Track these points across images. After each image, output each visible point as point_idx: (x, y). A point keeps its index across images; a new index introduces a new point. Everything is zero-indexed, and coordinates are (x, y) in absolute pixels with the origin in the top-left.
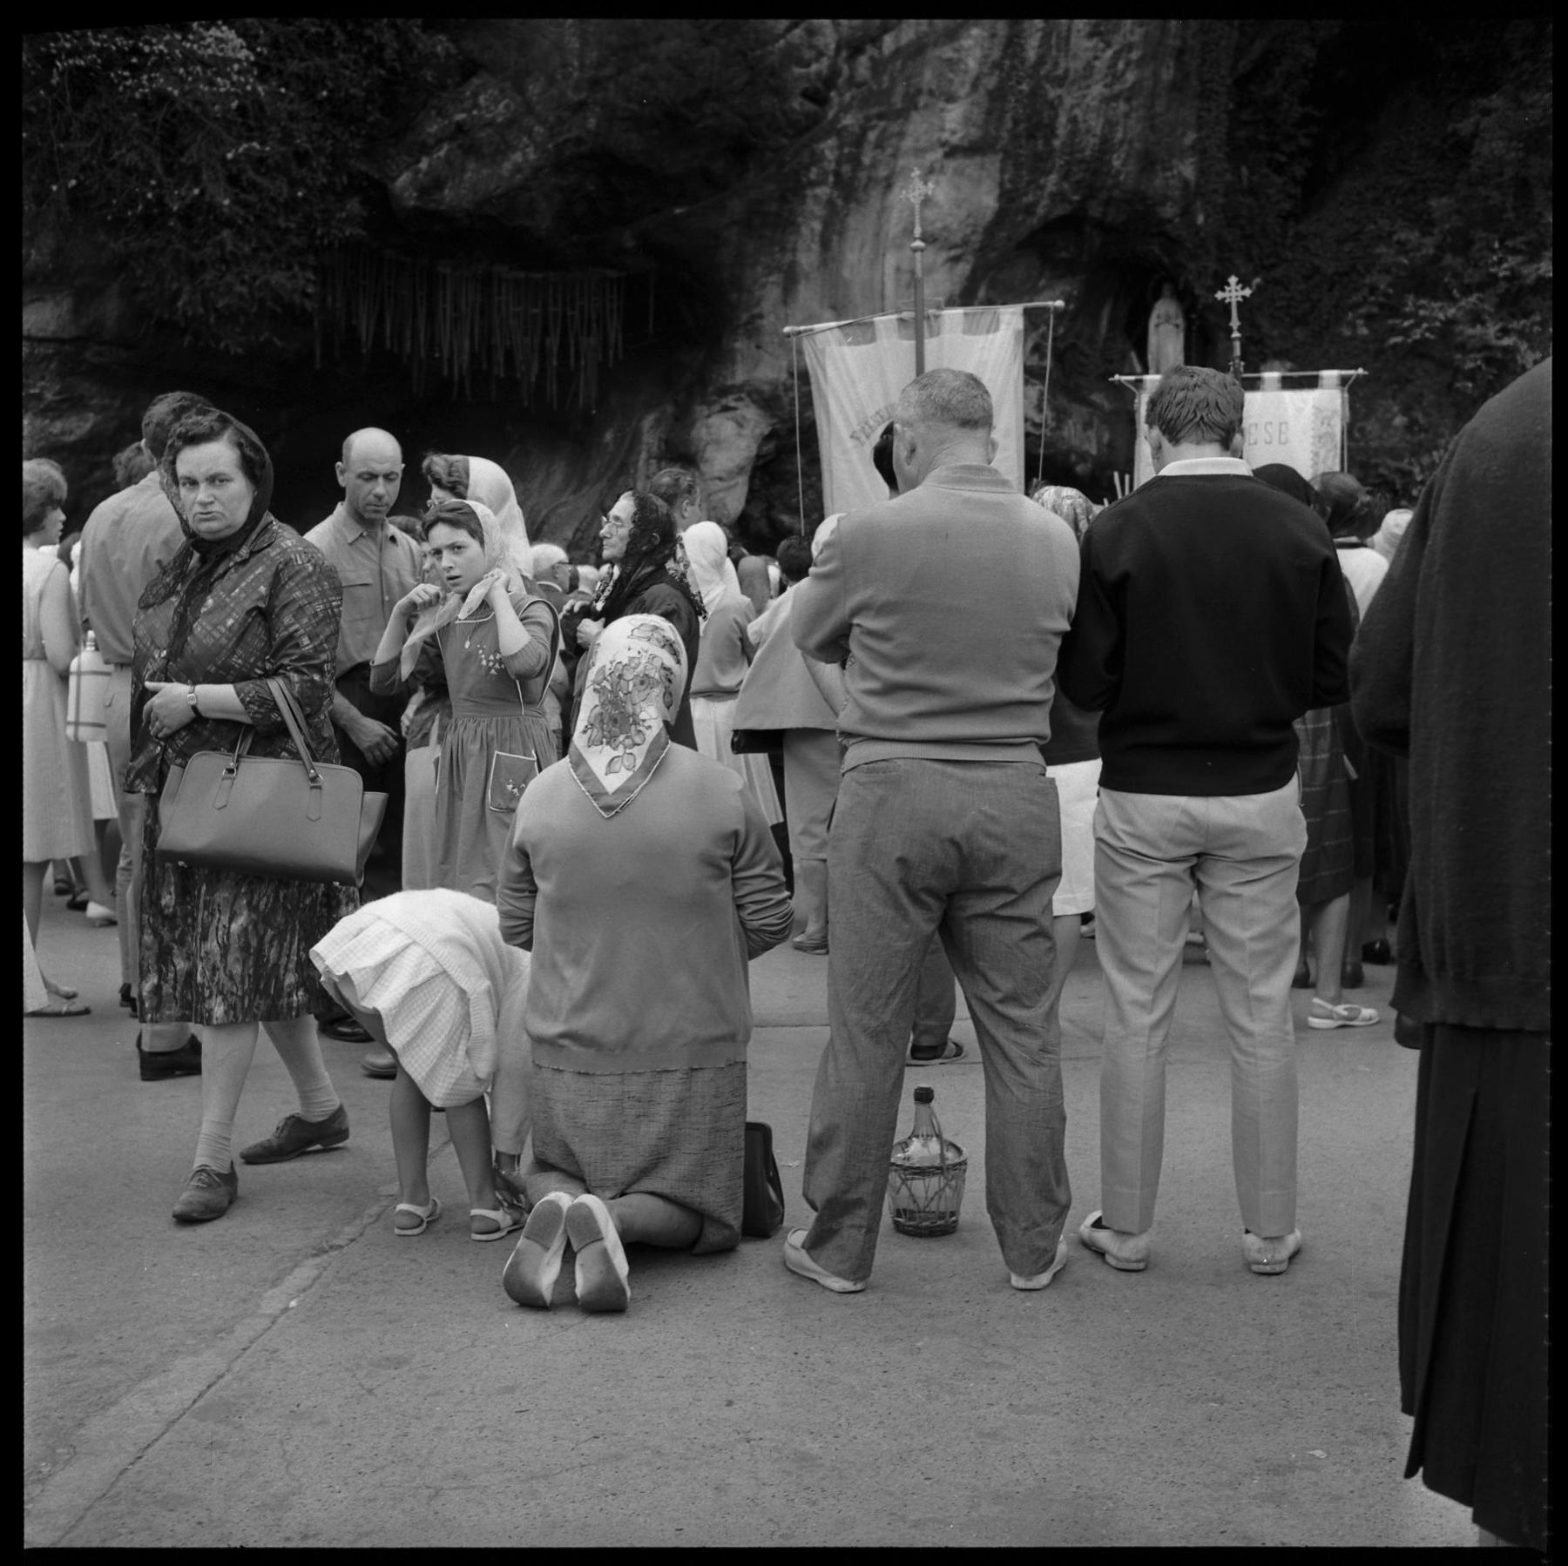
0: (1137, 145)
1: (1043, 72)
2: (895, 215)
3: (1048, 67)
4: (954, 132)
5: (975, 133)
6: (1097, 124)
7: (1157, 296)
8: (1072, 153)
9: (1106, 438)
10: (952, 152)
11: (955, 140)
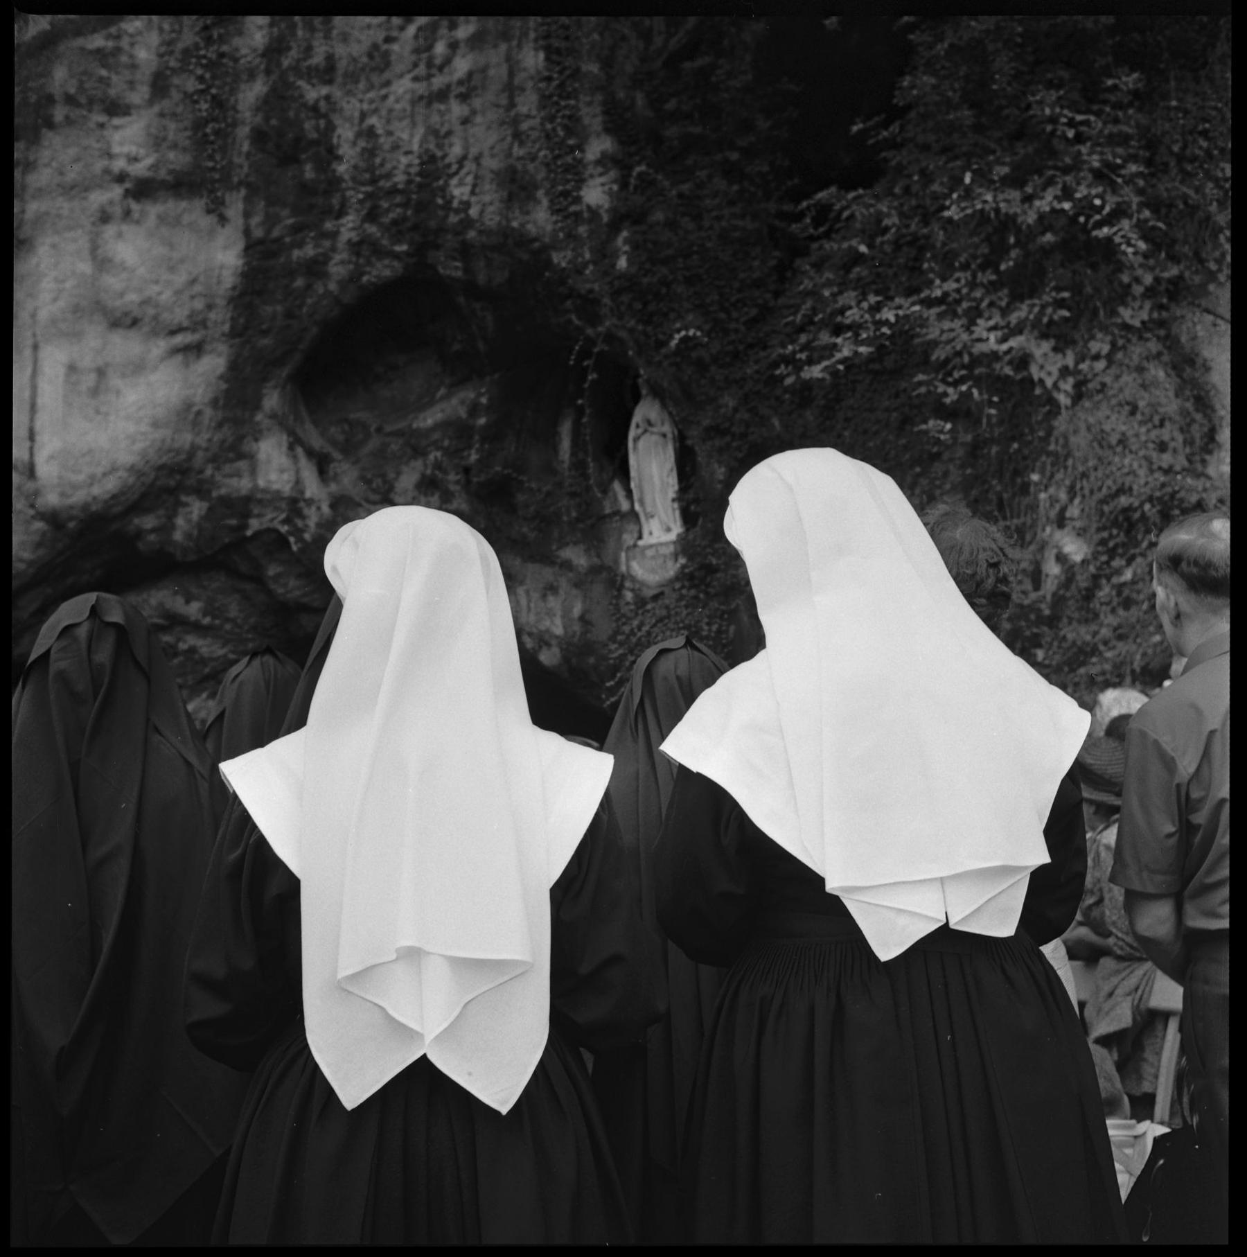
0: (491, 163)
1: (286, 63)
2: (47, 285)
3: (294, 53)
4: (134, 159)
5: (178, 160)
6: (413, 138)
7: (637, 399)
8: (373, 181)
9: (577, 610)
10: (143, 190)
11: (140, 169)
